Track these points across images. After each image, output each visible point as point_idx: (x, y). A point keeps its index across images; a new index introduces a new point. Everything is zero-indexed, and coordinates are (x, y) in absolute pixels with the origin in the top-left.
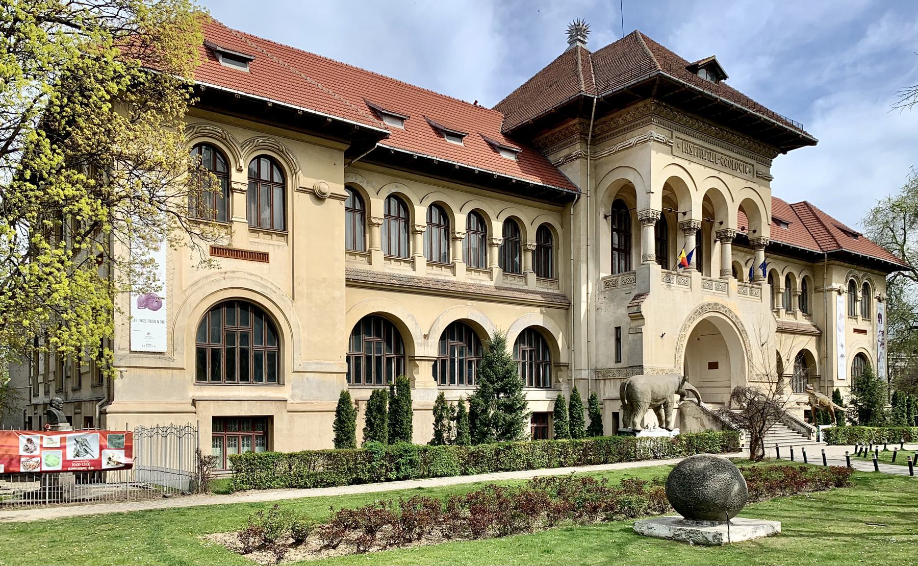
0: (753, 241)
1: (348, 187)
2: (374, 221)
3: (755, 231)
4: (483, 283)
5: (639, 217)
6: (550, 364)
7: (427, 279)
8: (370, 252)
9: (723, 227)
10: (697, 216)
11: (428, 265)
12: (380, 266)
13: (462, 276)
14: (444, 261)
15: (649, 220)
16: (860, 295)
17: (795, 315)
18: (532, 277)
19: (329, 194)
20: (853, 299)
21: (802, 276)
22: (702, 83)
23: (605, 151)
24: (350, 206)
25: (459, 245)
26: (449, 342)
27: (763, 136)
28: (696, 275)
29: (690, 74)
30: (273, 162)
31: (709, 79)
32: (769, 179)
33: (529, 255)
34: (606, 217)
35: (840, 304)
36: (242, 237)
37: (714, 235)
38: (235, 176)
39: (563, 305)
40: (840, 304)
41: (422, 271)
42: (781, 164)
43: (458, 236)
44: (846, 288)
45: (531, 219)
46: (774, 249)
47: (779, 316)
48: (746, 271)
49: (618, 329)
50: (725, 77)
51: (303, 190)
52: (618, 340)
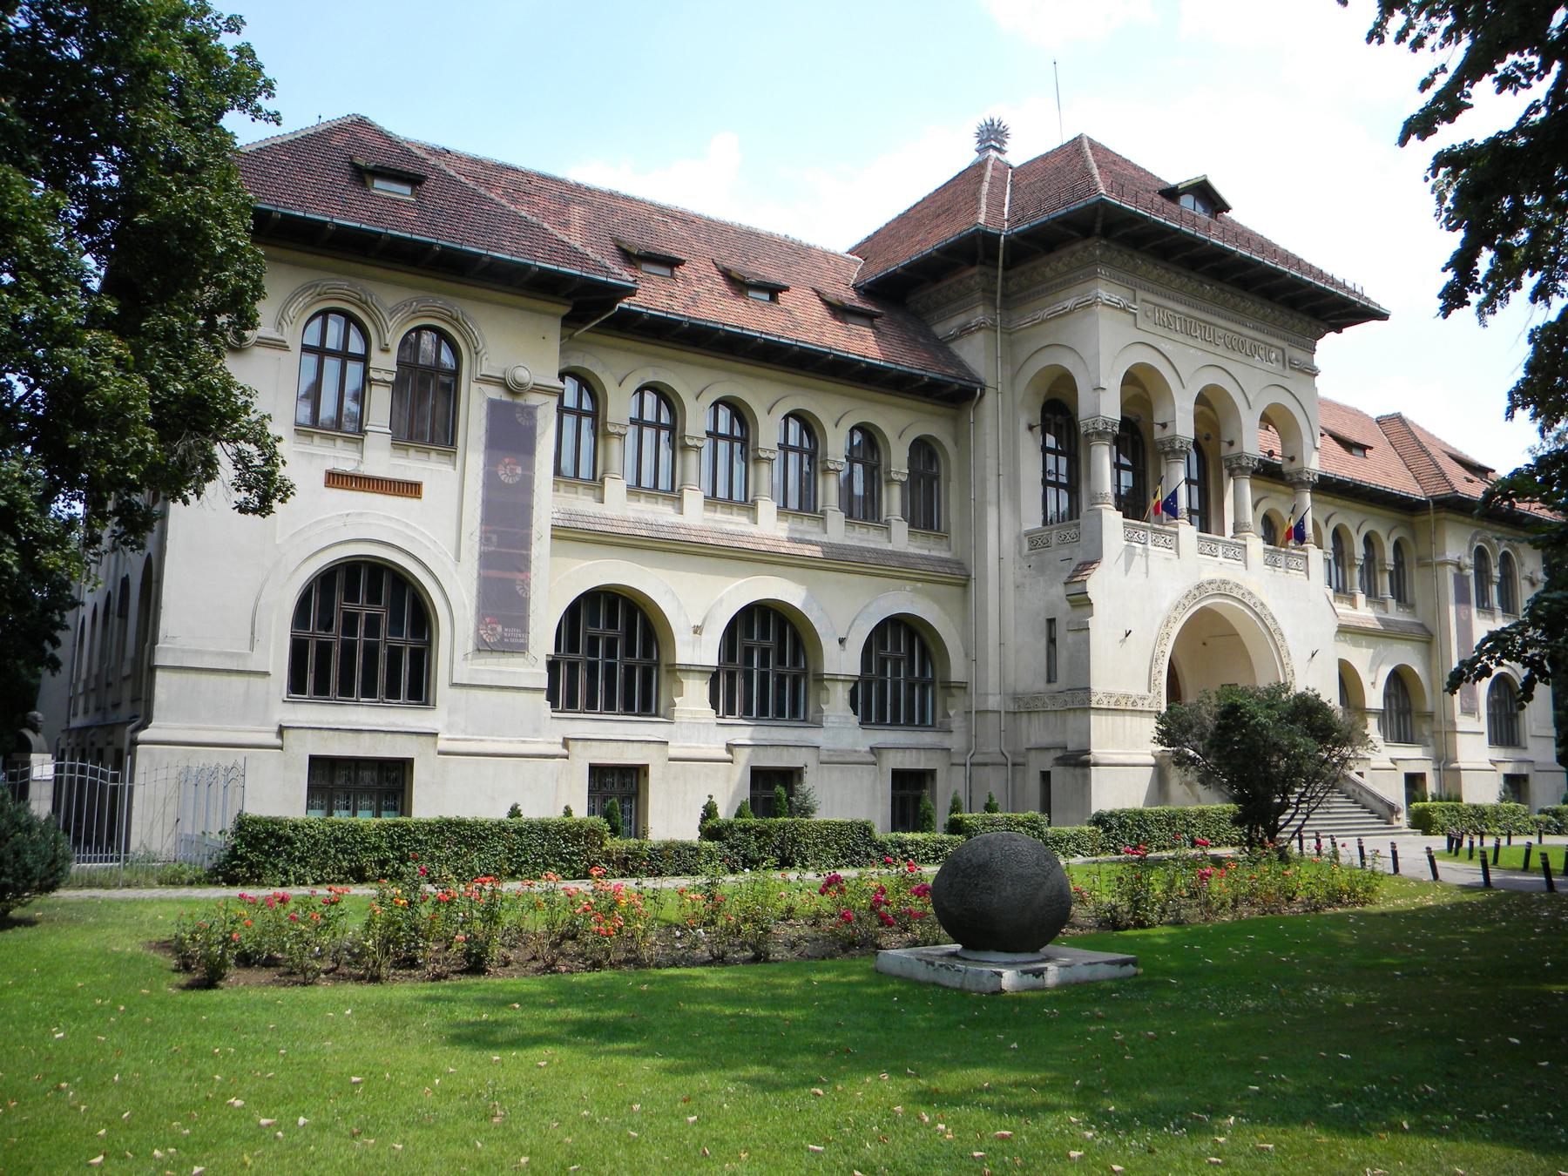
2: (611, 429)
3: (1292, 459)
5: (1083, 430)
6: (932, 682)
8: (602, 480)
10: (1185, 428)
12: (617, 506)
15: (1101, 435)
18: (900, 529)
21: (1393, 539)
28: (1188, 532)
32: (1313, 373)
33: (896, 491)
34: (1031, 428)
36: (380, 458)
39: (959, 578)
41: (694, 515)
42: (1332, 349)
43: (762, 455)
45: (900, 426)
46: (1329, 487)
52: (1052, 641)
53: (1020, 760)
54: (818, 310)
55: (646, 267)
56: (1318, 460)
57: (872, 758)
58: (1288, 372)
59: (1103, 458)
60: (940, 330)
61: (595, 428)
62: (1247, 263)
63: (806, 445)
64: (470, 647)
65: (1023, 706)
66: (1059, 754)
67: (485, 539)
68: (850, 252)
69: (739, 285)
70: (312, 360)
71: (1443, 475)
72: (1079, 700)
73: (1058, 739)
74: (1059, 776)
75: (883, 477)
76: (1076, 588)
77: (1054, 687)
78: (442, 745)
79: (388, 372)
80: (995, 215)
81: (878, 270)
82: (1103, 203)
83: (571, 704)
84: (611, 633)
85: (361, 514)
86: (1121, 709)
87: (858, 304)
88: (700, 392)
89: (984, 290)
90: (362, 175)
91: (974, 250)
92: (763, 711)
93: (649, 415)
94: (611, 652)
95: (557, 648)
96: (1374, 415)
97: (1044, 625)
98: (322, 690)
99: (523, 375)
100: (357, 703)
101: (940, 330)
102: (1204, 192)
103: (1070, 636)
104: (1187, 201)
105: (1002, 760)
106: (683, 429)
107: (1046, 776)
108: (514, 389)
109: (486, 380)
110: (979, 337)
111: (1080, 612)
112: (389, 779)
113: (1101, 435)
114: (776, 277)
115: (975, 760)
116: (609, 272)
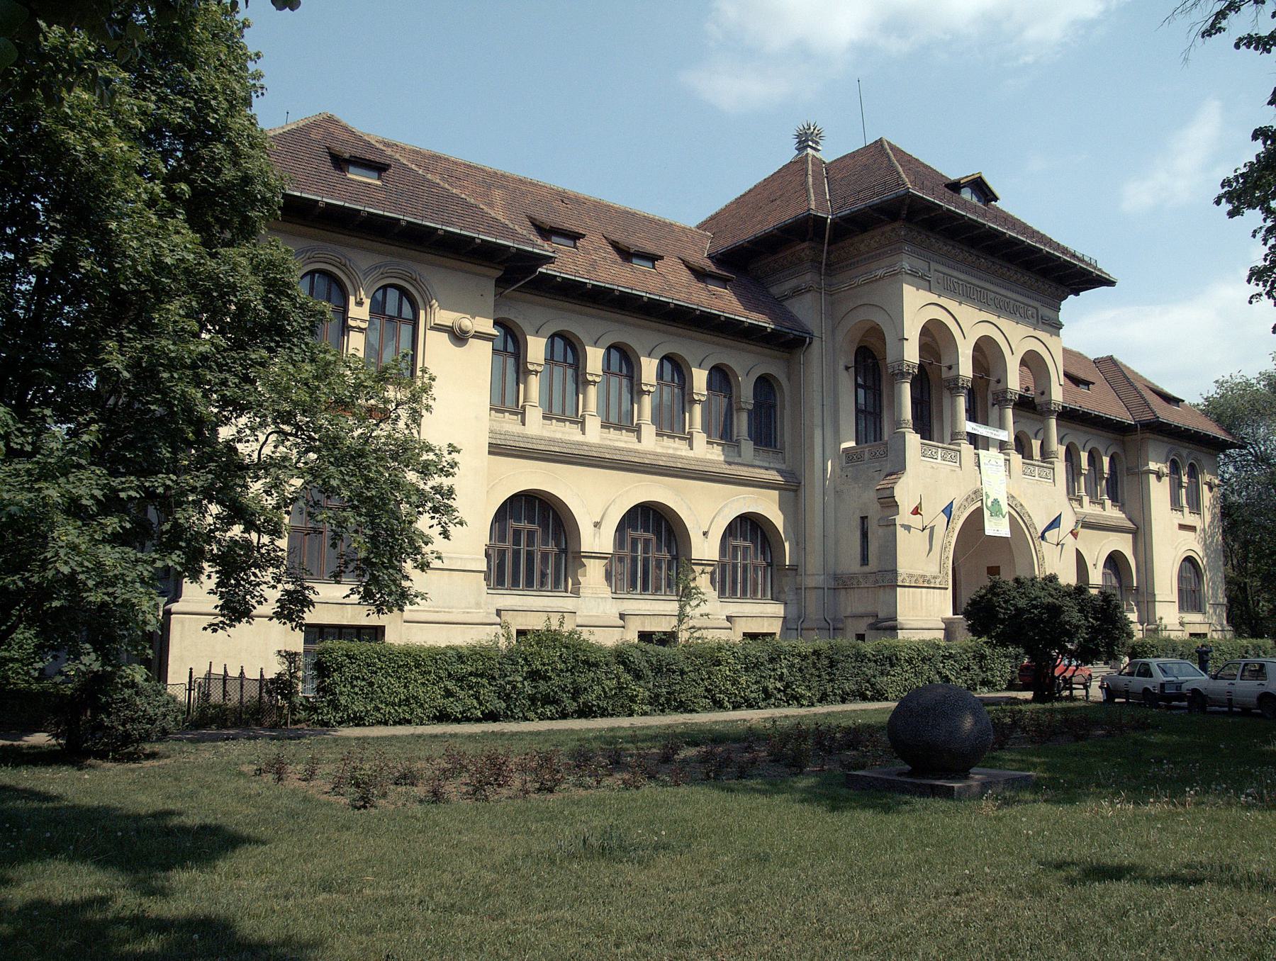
0: (1041, 405)
1: (497, 323)
3: (1043, 393)
8: (524, 407)
9: (1000, 387)
10: (966, 369)
11: (602, 427)
12: (536, 427)
13: (650, 443)
16: (1185, 479)
17: (1103, 505)
19: (472, 333)
20: (1176, 487)
25: (647, 401)
26: (630, 533)
27: (1047, 276)
29: (949, 193)
30: (403, 292)
33: (744, 416)
34: (847, 368)
35: (1159, 492)
37: (990, 397)
38: (354, 311)
40: (1159, 492)
41: (594, 434)
44: (1166, 470)
45: (747, 367)
46: (1069, 416)
47: (1081, 505)
48: (1036, 444)
50: (996, 199)
51: (439, 328)
53: (840, 626)
54: (686, 275)
59: (906, 391)
62: (1014, 242)
66: (871, 620)
68: (698, 227)
69: (626, 254)
71: (1148, 405)
72: (888, 579)
73: (870, 609)
77: (866, 569)
80: (820, 203)
81: (726, 243)
82: (908, 195)
83: (500, 582)
86: (924, 583)
87: (713, 268)
89: (812, 260)
90: (340, 162)
96: (1092, 357)
97: (859, 520)
101: (776, 290)
102: (980, 187)
103: (881, 531)
110: (808, 297)
111: (887, 512)
114: (650, 248)
115: (804, 626)
116: (534, 245)
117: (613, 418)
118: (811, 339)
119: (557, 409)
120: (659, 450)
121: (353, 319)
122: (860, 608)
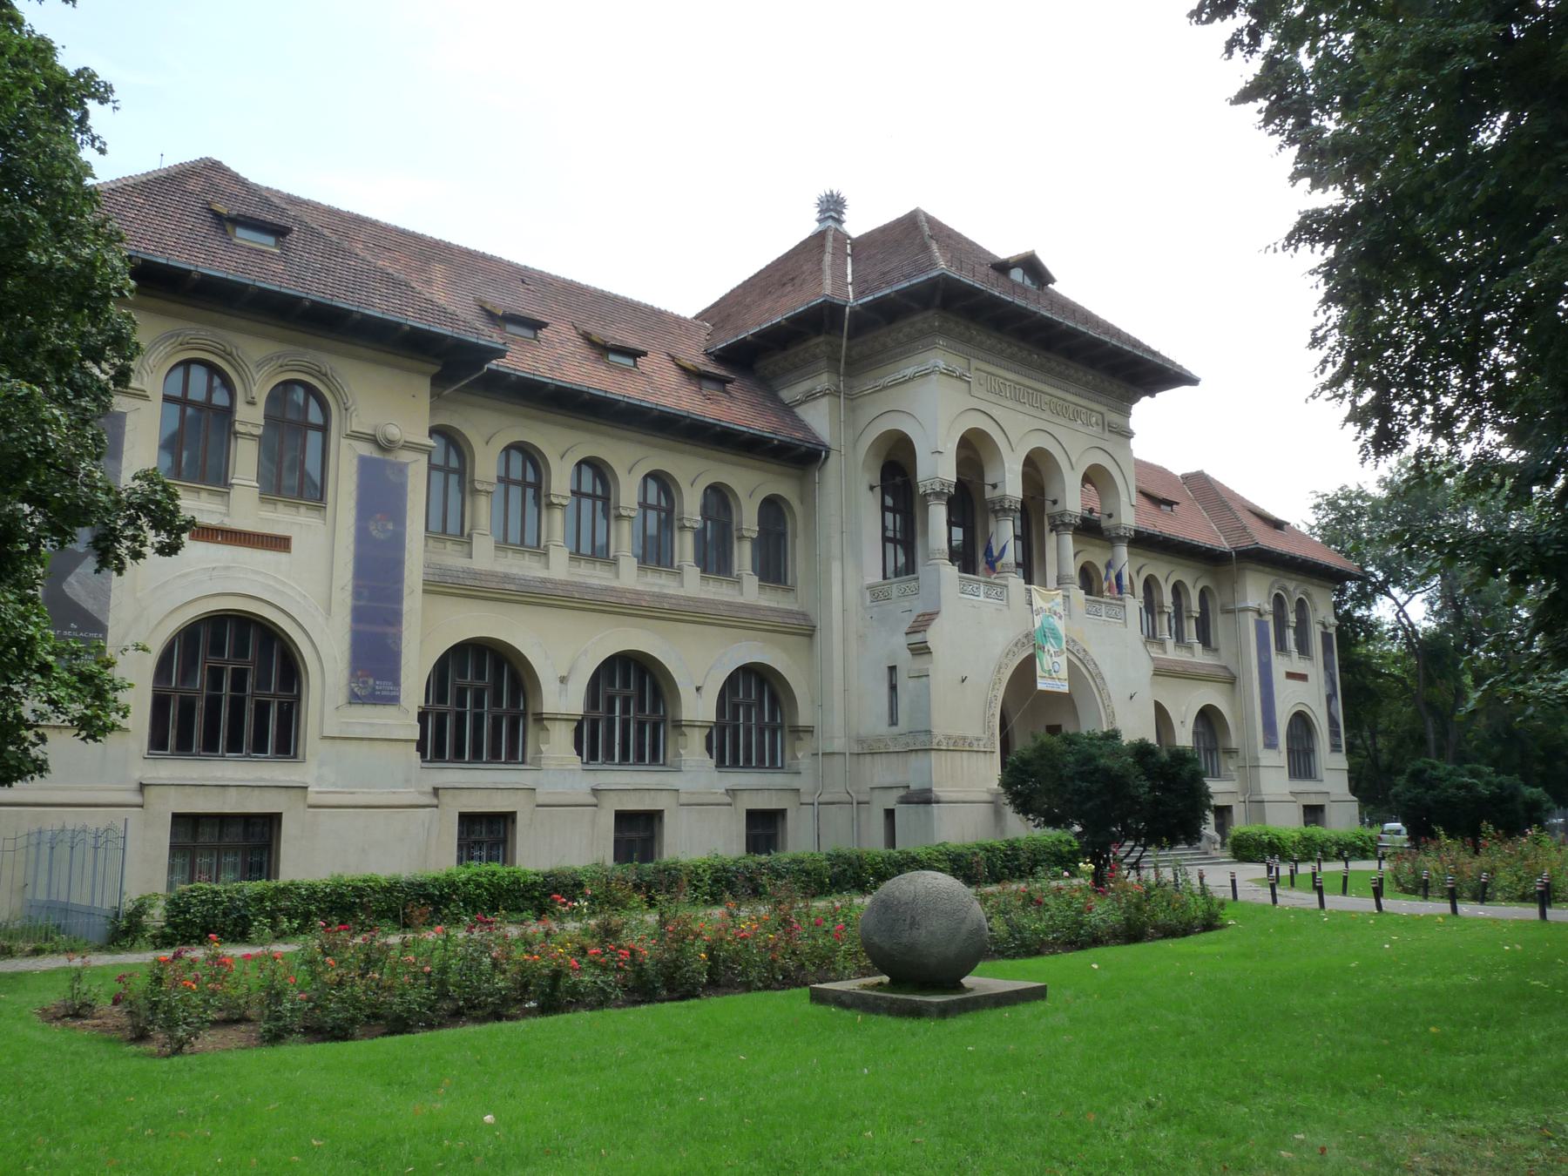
1: (434, 431)
3: (1110, 516)
4: (666, 591)
6: (782, 727)
7: (567, 583)
8: (470, 536)
10: (1013, 488)
12: (485, 557)
13: (629, 576)
14: (601, 555)
16: (1292, 618)
18: (751, 583)
21: (1199, 586)
22: (1015, 284)
23: (867, 383)
24: (438, 459)
28: (1016, 582)
31: (1028, 282)
32: (1127, 434)
34: (872, 488)
39: (805, 630)
41: (560, 567)
45: (752, 487)
46: (1144, 542)
49: (892, 669)
50: (1052, 281)
52: (893, 688)
54: (673, 377)
55: (511, 328)
56: (1129, 515)
57: (728, 799)
58: (1107, 435)
59: (938, 514)
60: (787, 395)
61: (462, 484)
63: (663, 503)
64: (342, 696)
65: (869, 750)
66: (902, 792)
67: (357, 594)
68: (696, 317)
69: (603, 349)
70: (176, 409)
73: (900, 779)
74: (902, 813)
75: (735, 534)
76: (917, 638)
77: (895, 730)
78: (312, 798)
79: (257, 426)
80: (842, 285)
83: (439, 755)
84: (479, 684)
85: (228, 568)
86: (961, 746)
88: (563, 449)
91: (821, 320)
92: (625, 756)
93: (516, 473)
94: (478, 702)
95: (427, 700)
98: (184, 747)
99: (394, 432)
100: (197, 757)
101: (787, 395)
102: (1032, 266)
103: (912, 683)
104: (1017, 275)
105: (847, 798)
106: (549, 487)
107: (890, 814)
108: (385, 446)
109: (356, 436)
112: (256, 836)
113: (938, 495)
114: (633, 342)
115: (822, 799)
117: (586, 548)
118: (828, 453)
119: (514, 536)
120: (640, 588)
121: (242, 423)
122: (888, 780)
